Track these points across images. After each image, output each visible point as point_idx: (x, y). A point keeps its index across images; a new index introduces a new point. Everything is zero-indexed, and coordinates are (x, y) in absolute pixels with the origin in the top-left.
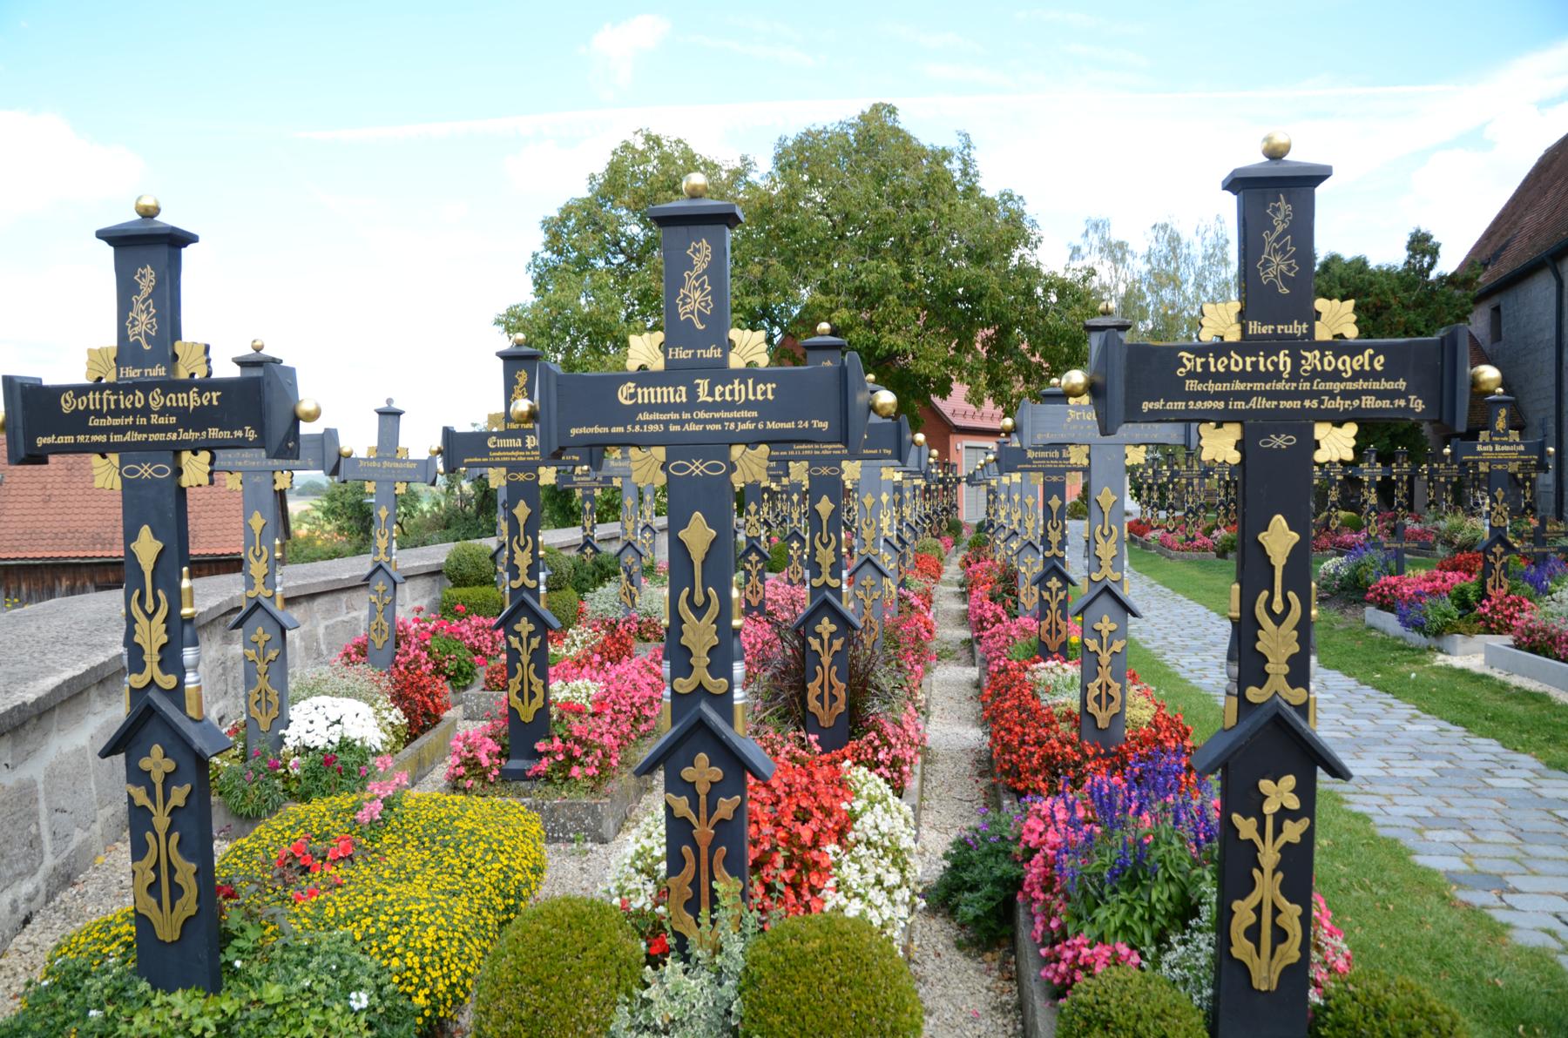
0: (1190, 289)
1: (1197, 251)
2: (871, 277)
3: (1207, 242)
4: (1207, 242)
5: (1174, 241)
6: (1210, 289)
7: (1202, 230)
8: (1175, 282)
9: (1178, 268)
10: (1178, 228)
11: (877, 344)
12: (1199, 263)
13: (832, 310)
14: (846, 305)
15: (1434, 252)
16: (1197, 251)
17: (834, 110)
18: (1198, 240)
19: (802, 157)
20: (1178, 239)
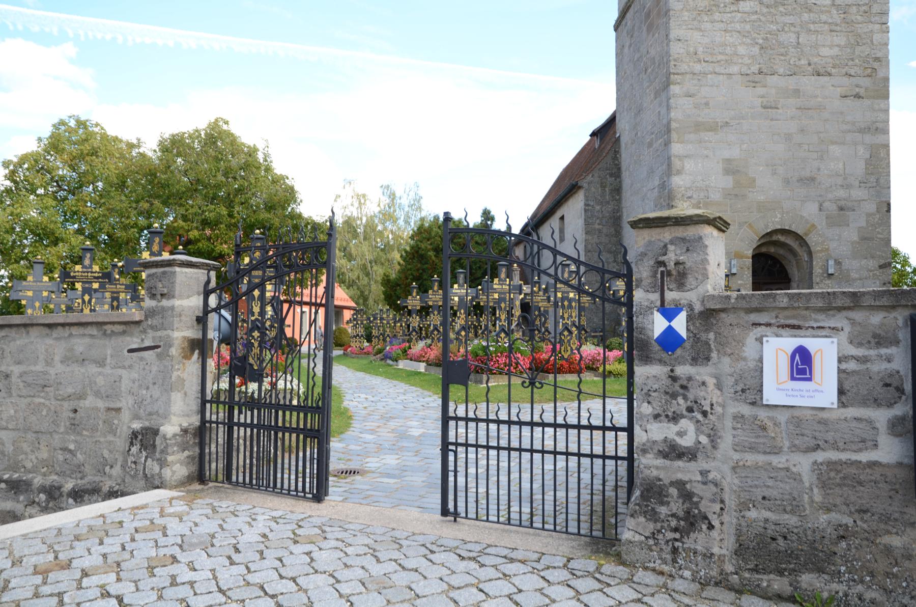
0: (401, 222)
1: (405, 202)
2: (211, 214)
3: (410, 197)
4: (410, 197)
5: (393, 196)
6: (412, 224)
7: (408, 190)
8: (395, 221)
9: (395, 211)
10: (393, 187)
11: (213, 250)
12: (406, 209)
13: (189, 231)
14: (197, 228)
15: (492, 219)
16: (405, 202)
17: (190, 119)
18: (405, 196)
19: (173, 146)
20: (394, 194)
